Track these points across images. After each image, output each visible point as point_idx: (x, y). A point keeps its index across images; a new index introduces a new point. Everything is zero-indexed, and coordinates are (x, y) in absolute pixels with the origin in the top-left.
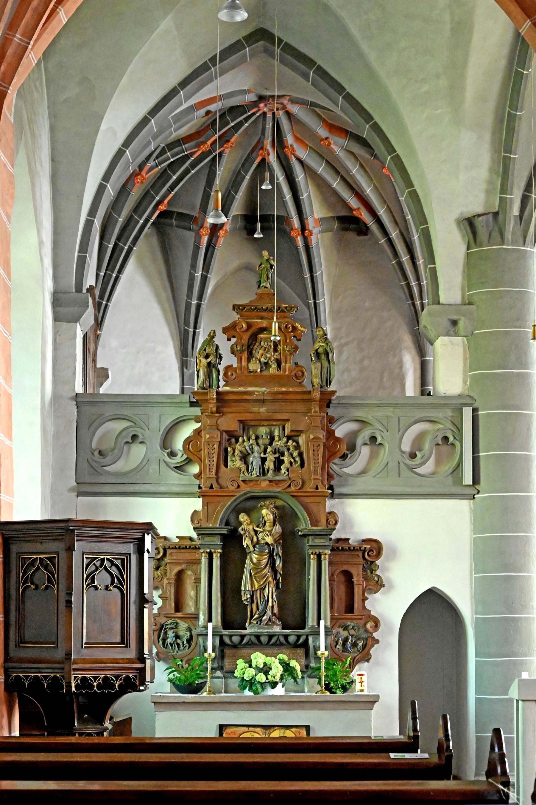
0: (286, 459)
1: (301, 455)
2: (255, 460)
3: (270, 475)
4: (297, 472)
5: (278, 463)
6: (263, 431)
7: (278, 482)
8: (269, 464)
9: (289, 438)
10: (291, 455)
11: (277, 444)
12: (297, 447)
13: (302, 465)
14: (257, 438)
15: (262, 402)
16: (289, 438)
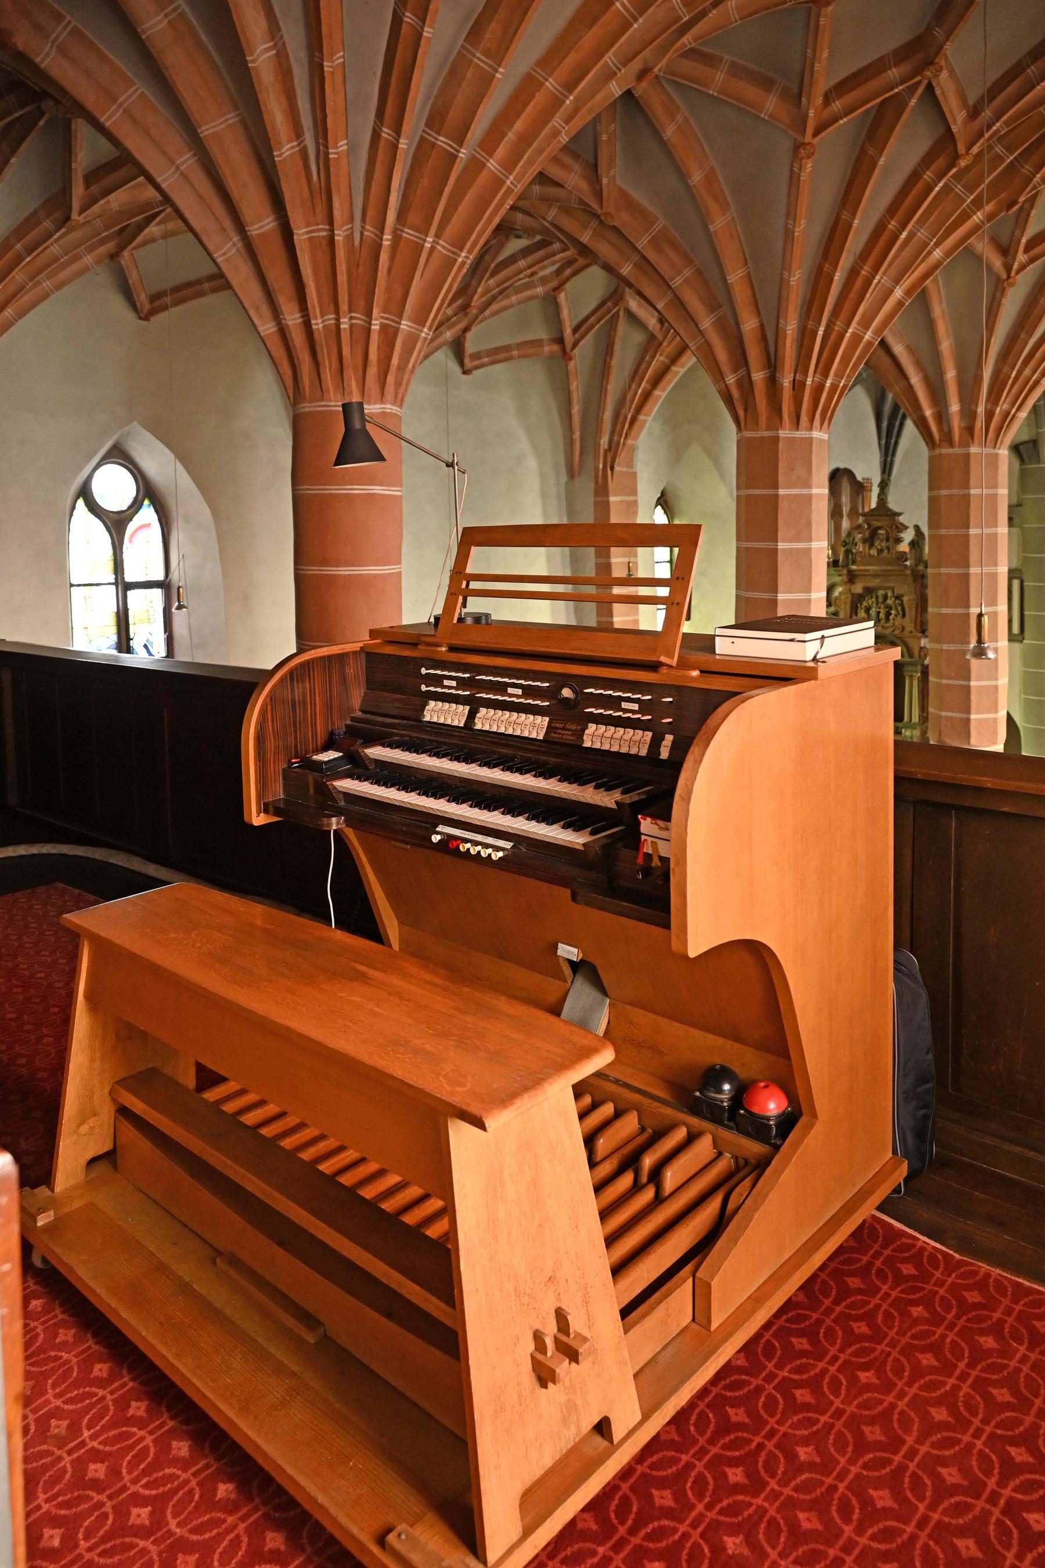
0: (893, 612)
1: (903, 610)
2: (873, 612)
3: (883, 622)
4: (899, 621)
5: (888, 614)
6: (881, 592)
7: (887, 628)
8: (882, 615)
9: (897, 598)
10: (897, 610)
11: (889, 602)
12: (902, 605)
13: (904, 616)
14: (877, 597)
15: (876, 575)
16: (897, 598)
